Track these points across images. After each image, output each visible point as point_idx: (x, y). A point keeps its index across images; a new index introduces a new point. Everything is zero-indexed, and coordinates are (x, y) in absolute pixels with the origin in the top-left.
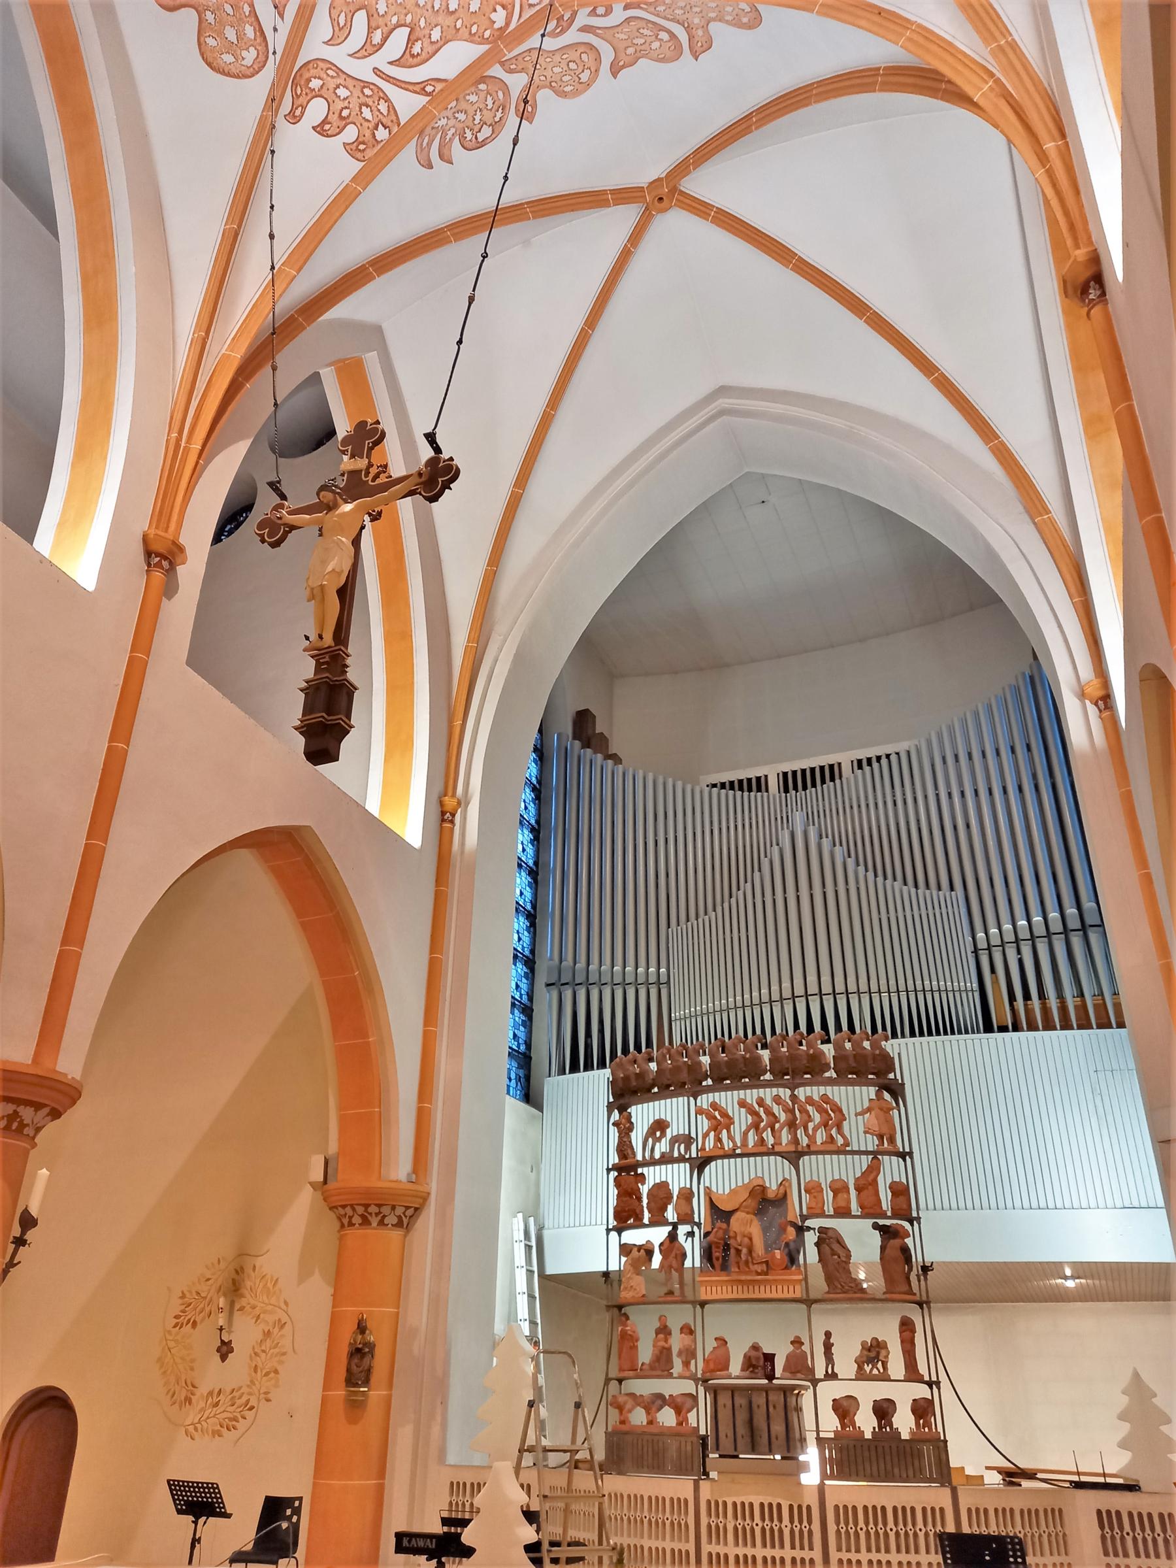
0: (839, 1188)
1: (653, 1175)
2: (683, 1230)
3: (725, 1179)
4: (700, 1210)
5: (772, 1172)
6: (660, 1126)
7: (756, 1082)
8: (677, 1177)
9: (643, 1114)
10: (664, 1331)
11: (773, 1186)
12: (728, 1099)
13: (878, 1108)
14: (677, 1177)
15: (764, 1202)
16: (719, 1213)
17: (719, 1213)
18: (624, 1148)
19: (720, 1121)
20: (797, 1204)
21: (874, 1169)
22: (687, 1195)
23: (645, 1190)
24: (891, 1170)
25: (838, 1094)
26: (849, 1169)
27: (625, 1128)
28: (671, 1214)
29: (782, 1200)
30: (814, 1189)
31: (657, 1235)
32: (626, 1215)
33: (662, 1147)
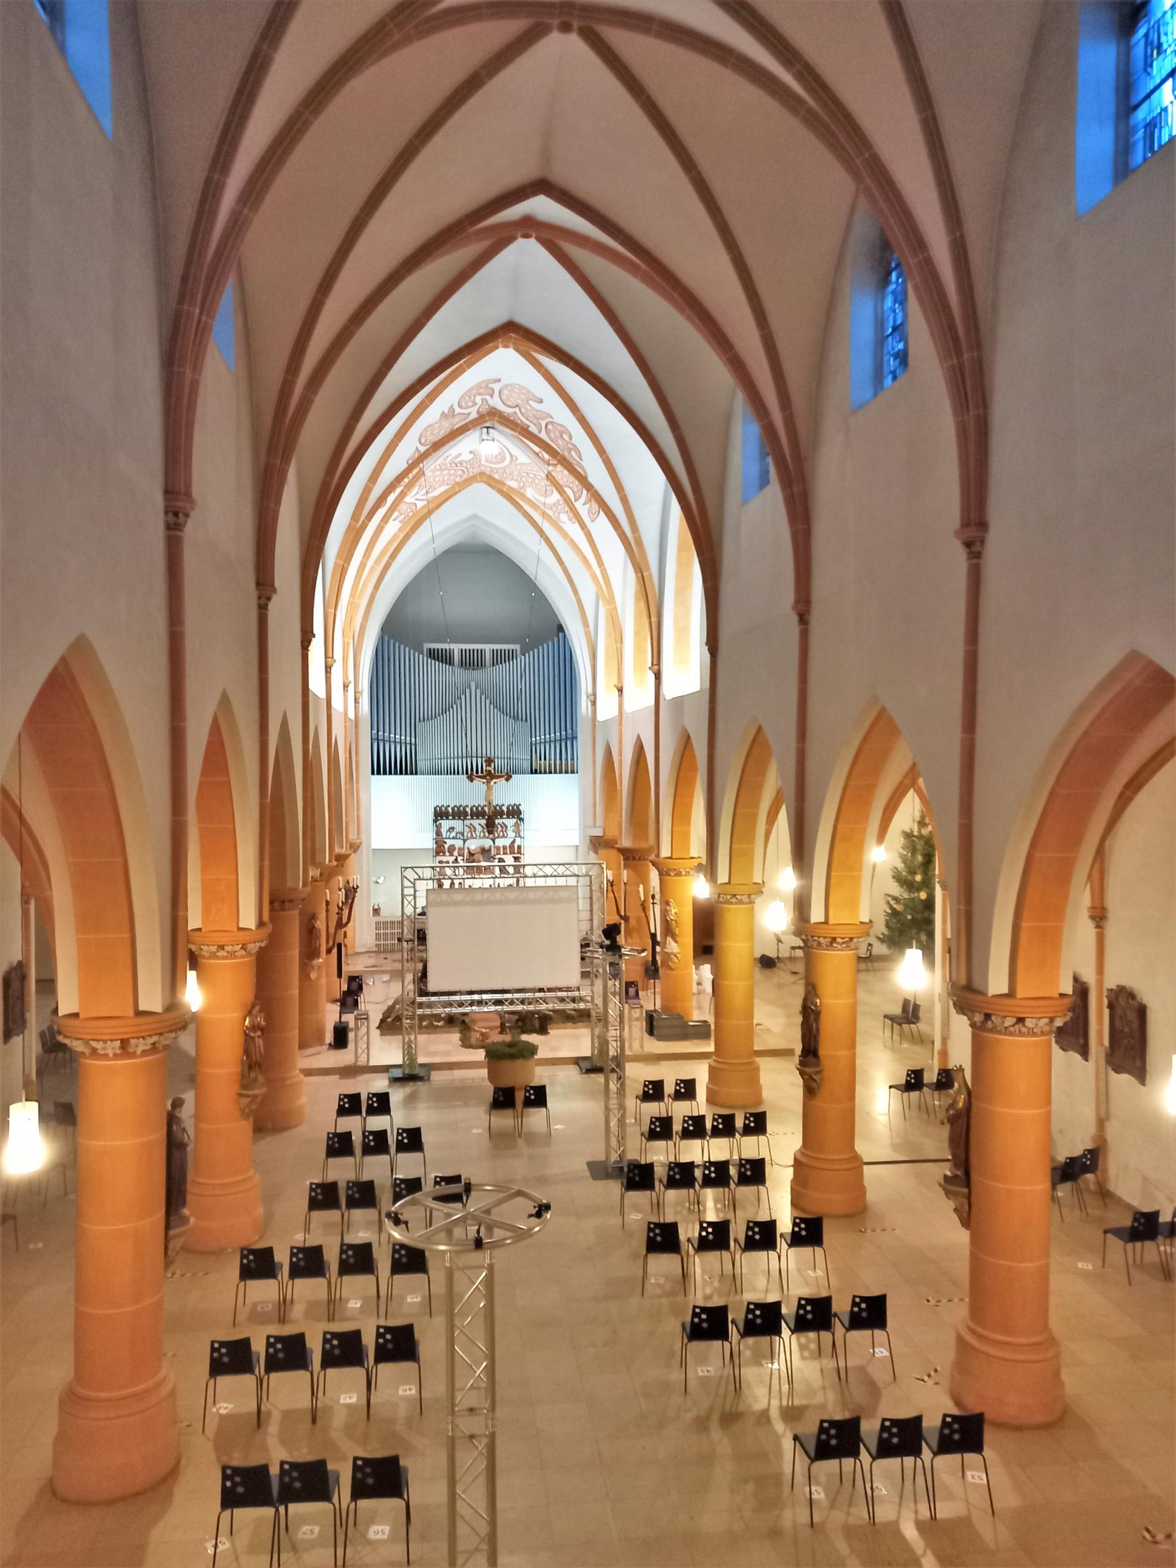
0: (505, 848)
1: (449, 842)
2: (460, 858)
3: (473, 845)
4: (466, 852)
5: (487, 843)
8: (458, 843)
11: (487, 847)
12: (476, 822)
13: (517, 825)
14: (458, 843)
16: (471, 854)
17: (471, 854)
18: (438, 833)
19: (472, 828)
20: (493, 852)
21: (514, 842)
23: (446, 846)
24: (518, 840)
25: (507, 821)
27: (438, 828)
28: (456, 853)
29: (489, 850)
30: (498, 848)
31: (452, 859)
33: (453, 834)
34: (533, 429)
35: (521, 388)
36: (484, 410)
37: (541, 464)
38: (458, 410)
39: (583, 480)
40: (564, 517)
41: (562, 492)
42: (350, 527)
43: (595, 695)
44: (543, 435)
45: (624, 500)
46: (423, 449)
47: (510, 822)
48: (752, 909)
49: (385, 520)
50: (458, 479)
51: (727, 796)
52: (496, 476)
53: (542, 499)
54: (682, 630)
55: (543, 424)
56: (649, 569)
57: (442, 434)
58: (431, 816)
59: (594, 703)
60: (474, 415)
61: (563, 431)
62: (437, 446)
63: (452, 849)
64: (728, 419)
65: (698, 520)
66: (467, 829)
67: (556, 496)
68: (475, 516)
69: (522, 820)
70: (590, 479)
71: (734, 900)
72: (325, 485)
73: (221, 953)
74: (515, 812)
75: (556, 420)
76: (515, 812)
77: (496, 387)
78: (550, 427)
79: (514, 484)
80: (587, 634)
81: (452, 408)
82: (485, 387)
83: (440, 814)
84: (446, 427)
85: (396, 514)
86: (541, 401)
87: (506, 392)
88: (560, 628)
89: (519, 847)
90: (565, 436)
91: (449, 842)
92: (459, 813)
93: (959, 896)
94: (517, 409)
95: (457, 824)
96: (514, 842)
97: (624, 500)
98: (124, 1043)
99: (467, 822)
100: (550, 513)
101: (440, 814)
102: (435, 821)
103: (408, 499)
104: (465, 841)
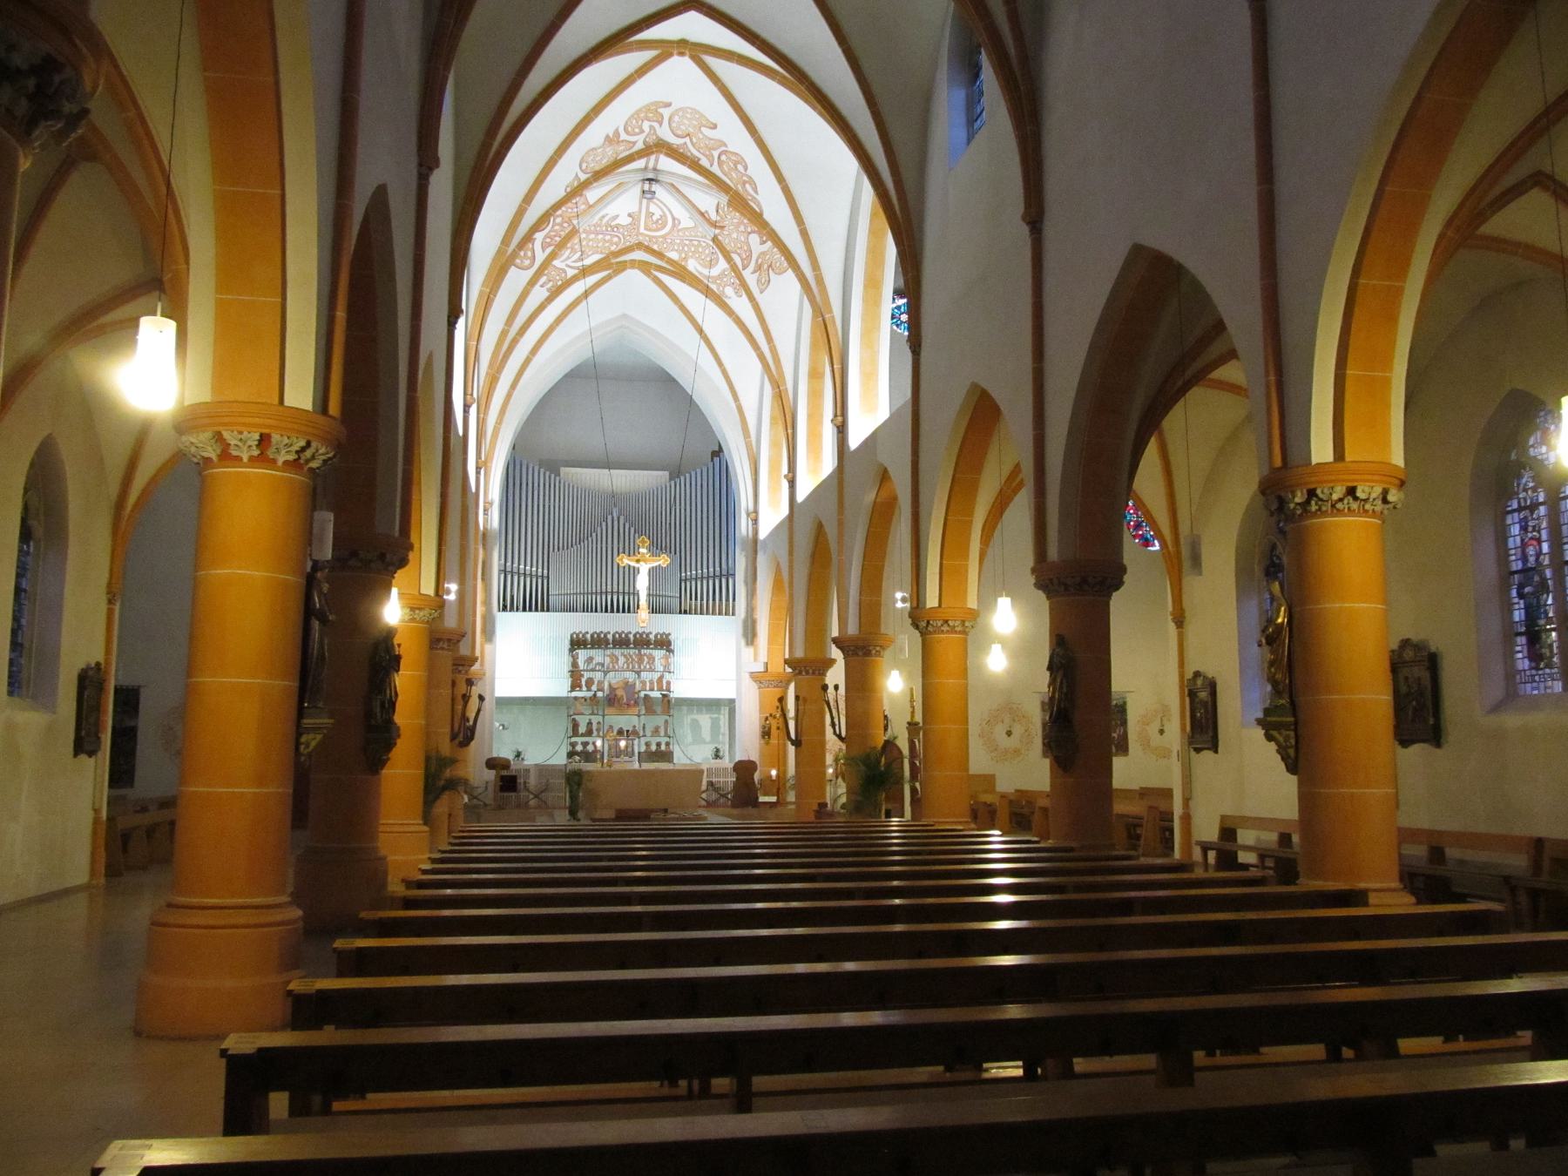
1: (586, 675)
3: (614, 679)
5: (631, 676)
6: (590, 659)
7: (628, 646)
8: (598, 676)
9: (582, 654)
10: (590, 723)
14: (598, 676)
15: (628, 686)
18: (575, 664)
20: (638, 686)
21: (661, 678)
22: (600, 683)
26: (656, 676)
28: (594, 688)
32: (575, 685)
34: (704, 162)
35: (695, 111)
36: (651, 141)
37: (707, 227)
38: (623, 136)
39: (757, 220)
40: (729, 291)
41: (729, 259)
42: (500, 252)
43: (756, 511)
44: (715, 169)
45: (804, 233)
46: (583, 177)
47: (658, 654)
48: (966, 641)
49: (532, 283)
50: (613, 248)
51: (934, 513)
52: (655, 247)
53: (706, 272)
54: (869, 376)
55: (716, 154)
56: (831, 311)
57: (605, 162)
58: (567, 645)
59: (755, 521)
60: (640, 146)
61: (739, 160)
62: (598, 175)
63: (590, 682)
64: (927, 99)
65: (897, 208)
66: (608, 660)
67: (722, 264)
68: (624, 316)
69: (670, 651)
70: (765, 216)
71: (945, 628)
72: (486, 146)
73: (352, 562)
74: (664, 643)
75: (730, 149)
76: (664, 643)
77: (666, 112)
78: (723, 158)
79: (674, 255)
80: (748, 445)
81: (617, 133)
82: (653, 111)
83: (577, 643)
84: (610, 154)
85: (544, 279)
86: (715, 127)
87: (676, 118)
88: (718, 453)
89: (669, 683)
90: (740, 167)
91: (586, 675)
92: (599, 642)
93: (1266, 357)
94: (687, 140)
95: (598, 655)
96: (661, 678)
97: (804, 233)
98: (264, 440)
99: (608, 652)
100: (713, 287)
101: (577, 643)
102: (572, 650)
103: (556, 263)
104: (606, 673)
